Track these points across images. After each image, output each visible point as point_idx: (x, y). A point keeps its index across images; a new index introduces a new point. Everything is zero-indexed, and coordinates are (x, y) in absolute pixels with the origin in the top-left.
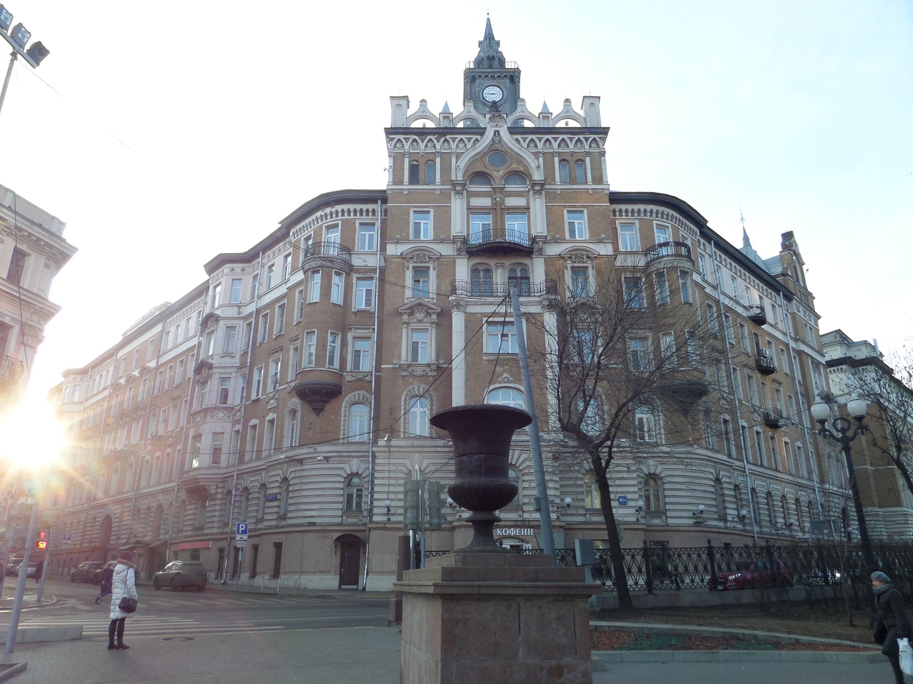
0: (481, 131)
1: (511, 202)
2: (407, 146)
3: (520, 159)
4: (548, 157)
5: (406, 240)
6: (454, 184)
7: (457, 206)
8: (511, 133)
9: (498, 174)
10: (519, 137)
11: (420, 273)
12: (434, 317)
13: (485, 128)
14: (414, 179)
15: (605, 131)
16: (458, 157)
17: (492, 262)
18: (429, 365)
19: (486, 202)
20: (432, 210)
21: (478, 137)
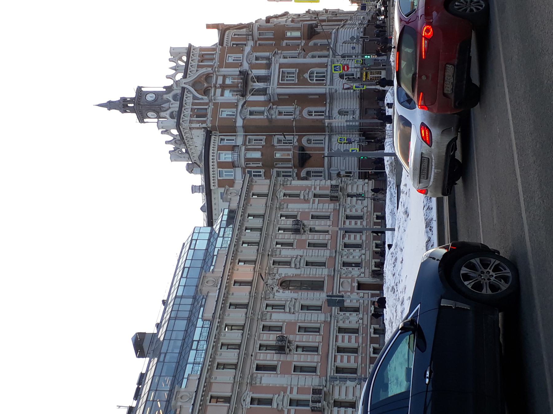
0: (183, 89)
1: (220, 81)
2: (186, 119)
3: (200, 77)
4: (199, 66)
5: (235, 119)
6: (210, 101)
7: (220, 99)
8: (186, 78)
9: (206, 85)
10: (188, 76)
11: (251, 113)
12: (274, 107)
13: (182, 87)
14: (205, 116)
15: (190, 46)
16: (195, 98)
17: (250, 88)
18: (295, 109)
19: (219, 91)
20: (221, 109)
21: (186, 91)
